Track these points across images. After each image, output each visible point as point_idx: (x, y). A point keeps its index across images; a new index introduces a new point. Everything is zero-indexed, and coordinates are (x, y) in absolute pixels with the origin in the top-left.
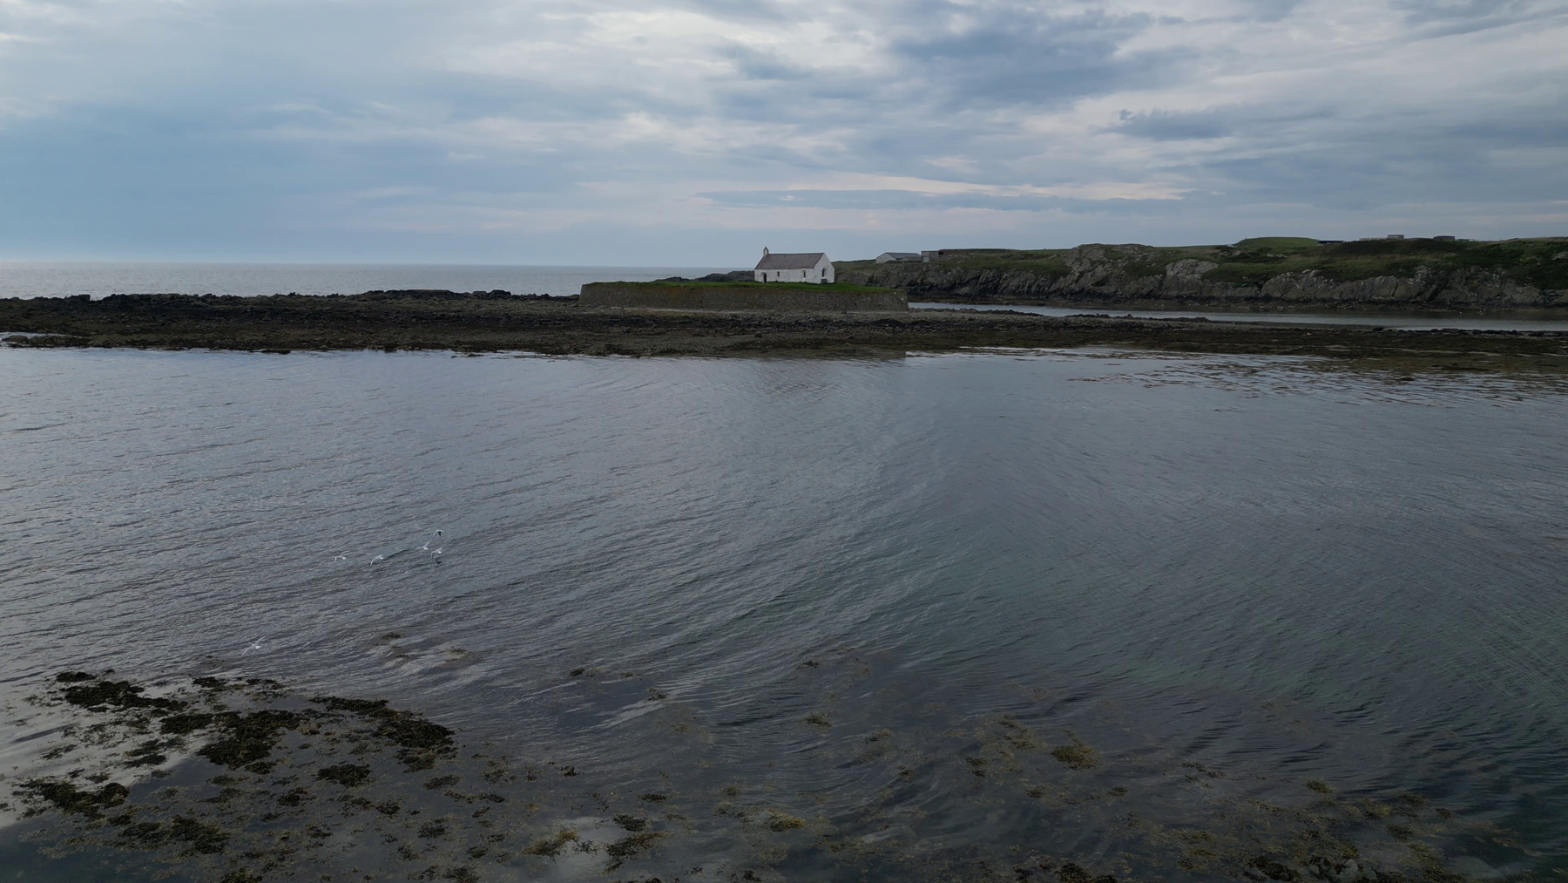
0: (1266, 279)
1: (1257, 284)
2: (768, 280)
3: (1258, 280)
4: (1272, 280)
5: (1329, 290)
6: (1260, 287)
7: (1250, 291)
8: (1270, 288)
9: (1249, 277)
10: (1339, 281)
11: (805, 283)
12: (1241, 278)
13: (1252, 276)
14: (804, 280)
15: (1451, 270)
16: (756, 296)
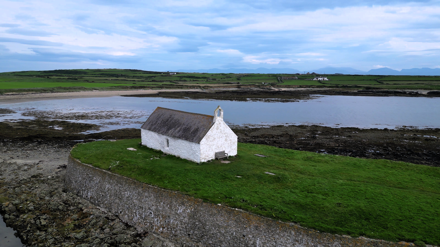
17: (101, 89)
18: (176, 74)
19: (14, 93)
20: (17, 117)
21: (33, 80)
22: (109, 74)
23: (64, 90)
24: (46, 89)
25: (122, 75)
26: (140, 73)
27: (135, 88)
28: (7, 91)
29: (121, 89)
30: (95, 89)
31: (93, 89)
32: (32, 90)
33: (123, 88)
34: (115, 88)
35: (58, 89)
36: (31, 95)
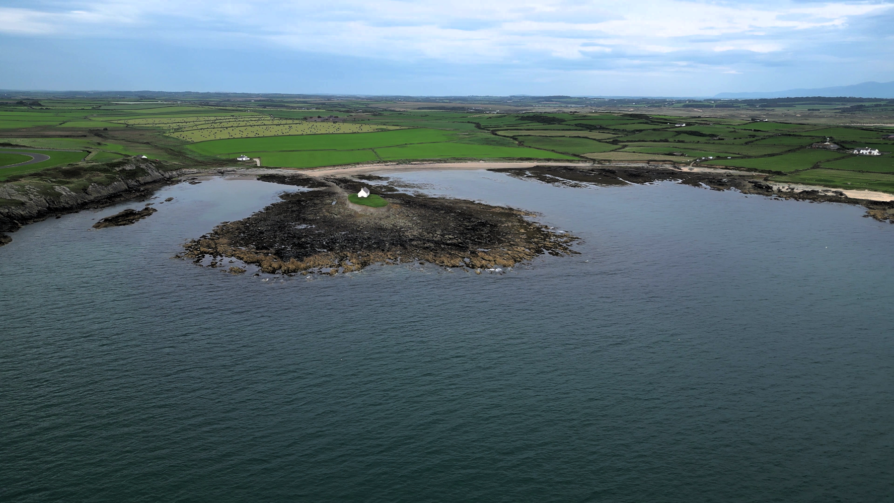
0: (86, 190)
17: (488, 160)
18: (684, 125)
19: (418, 162)
20: (385, 183)
21: (470, 141)
22: (586, 125)
23: (455, 161)
24: (442, 159)
25: (601, 127)
26: (634, 123)
27: (522, 160)
28: (414, 161)
29: (506, 161)
30: (483, 161)
31: (481, 160)
32: (431, 161)
33: (510, 160)
34: (502, 159)
35: (451, 159)
36: (428, 165)
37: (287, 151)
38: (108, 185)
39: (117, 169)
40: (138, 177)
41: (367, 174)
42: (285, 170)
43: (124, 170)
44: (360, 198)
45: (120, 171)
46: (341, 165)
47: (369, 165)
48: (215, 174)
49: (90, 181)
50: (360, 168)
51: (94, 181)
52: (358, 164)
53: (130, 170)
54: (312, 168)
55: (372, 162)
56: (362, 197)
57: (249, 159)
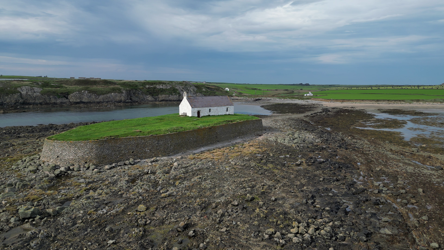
0: (68, 95)
1: (65, 97)
2: (202, 115)
3: (66, 95)
4: (72, 95)
5: (98, 98)
6: (67, 98)
7: (64, 100)
8: (72, 98)
9: (61, 94)
10: (99, 95)
11: (229, 115)
12: (58, 94)
13: (62, 93)
14: (228, 113)
15: (130, 91)
16: (240, 127)
37: (367, 93)
38: (103, 94)
39: (147, 86)
40: (162, 95)
41: (409, 110)
42: (313, 101)
43: (155, 88)
44: (181, 115)
45: (149, 88)
46: (388, 100)
47: (435, 103)
48: (247, 101)
49: (86, 89)
50: (416, 105)
51: (89, 89)
52: (418, 101)
53: (161, 89)
54: (343, 101)
55: (442, 101)
56: (185, 116)
57: (312, 95)
